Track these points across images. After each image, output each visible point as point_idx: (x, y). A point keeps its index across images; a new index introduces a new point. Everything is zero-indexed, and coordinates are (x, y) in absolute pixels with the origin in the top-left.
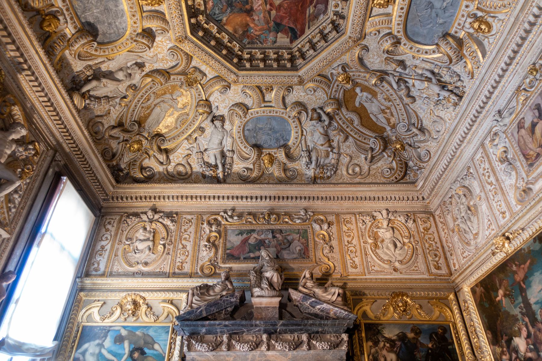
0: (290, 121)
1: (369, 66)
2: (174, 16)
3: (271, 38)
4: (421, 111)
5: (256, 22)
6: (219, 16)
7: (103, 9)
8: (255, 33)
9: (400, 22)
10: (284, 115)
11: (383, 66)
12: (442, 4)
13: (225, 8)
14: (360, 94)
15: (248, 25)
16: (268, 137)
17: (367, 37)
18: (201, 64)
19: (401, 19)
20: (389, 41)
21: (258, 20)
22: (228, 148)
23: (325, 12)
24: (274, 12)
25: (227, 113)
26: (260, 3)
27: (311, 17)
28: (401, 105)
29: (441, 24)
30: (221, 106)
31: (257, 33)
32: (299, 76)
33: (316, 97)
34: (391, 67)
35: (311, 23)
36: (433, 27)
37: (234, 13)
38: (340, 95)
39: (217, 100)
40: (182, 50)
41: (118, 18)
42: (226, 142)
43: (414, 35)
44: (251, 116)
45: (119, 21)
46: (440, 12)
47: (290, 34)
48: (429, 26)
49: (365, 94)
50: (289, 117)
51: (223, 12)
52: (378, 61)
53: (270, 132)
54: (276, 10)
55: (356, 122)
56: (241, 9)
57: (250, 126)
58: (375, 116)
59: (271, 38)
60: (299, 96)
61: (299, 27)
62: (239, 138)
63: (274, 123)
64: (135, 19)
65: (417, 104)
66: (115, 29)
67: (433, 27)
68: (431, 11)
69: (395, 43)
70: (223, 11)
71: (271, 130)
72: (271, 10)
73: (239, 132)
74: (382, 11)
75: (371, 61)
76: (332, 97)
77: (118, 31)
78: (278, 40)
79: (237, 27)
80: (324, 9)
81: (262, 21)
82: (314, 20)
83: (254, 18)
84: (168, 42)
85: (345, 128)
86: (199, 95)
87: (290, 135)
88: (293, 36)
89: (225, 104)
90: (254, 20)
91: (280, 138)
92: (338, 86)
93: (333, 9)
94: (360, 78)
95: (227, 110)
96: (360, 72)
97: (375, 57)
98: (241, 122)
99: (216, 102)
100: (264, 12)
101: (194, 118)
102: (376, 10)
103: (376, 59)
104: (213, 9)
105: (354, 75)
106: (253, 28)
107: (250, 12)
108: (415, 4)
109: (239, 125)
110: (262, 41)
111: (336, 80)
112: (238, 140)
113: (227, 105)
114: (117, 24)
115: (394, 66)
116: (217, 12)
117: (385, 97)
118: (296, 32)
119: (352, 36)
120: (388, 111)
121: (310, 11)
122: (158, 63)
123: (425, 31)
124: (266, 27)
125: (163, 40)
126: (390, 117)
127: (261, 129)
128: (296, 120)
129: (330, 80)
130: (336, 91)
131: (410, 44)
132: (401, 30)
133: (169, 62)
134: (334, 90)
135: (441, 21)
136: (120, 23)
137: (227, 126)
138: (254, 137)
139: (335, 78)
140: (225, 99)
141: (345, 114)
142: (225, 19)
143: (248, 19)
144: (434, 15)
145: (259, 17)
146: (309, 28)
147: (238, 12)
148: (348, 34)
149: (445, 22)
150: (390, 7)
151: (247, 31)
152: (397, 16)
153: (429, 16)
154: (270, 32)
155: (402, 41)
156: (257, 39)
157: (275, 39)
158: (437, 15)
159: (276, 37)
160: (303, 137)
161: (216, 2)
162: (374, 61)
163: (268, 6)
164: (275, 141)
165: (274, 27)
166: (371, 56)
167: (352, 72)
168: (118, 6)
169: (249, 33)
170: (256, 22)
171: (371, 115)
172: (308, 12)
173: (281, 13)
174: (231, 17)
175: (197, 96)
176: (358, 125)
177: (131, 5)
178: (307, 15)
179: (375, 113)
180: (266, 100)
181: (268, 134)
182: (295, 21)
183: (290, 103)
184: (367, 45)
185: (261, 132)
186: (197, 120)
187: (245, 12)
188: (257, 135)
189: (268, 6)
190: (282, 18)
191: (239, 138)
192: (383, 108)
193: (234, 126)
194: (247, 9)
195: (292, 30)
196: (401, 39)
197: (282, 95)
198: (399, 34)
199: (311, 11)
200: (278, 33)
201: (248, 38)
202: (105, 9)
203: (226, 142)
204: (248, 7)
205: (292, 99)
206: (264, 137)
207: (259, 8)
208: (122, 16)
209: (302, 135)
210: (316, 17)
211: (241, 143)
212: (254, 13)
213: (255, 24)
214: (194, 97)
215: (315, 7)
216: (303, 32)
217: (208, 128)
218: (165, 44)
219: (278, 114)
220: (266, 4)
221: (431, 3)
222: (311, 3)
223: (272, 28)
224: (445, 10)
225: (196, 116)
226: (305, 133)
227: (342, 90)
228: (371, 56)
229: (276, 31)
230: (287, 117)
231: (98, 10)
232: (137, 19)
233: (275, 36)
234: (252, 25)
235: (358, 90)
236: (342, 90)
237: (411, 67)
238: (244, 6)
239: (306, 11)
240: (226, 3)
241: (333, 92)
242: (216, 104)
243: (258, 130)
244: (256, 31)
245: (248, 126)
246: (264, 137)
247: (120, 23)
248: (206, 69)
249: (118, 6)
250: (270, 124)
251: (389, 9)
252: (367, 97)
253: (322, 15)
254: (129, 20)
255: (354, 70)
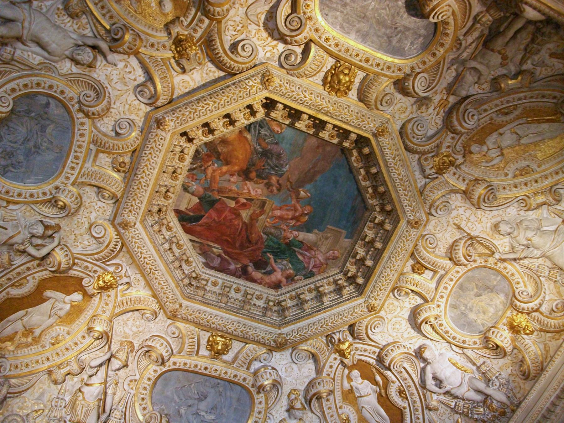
0: (48, 187)
1: (120, 318)
2: (306, 94)
3: (194, 186)
4: (37, 395)
5: (227, 177)
6: (255, 132)
7: (368, 14)
8: (210, 168)
9: (188, 366)
10: (62, 179)
11: (119, 338)
12: (203, 411)
13: (264, 145)
14: (68, 298)
15: (227, 164)
16: (21, 138)
17: (170, 321)
18: (205, 75)
19: (192, 366)
20: (167, 354)
21: (229, 181)
22: (18, 52)
23: (207, 265)
24: (232, 204)
25: (95, 76)
26: (252, 192)
27: (206, 247)
28: (47, 364)
29: (179, 412)
30: (115, 72)
31: (210, 171)
32: (135, 224)
33: (81, 235)
34: (115, 347)
35: (198, 245)
36: (175, 402)
37: (252, 154)
38: (74, 272)
39: (128, 70)
40: (248, 69)
41: (344, 20)
42: (33, 52)
43: (165, 379)
44: (77, 122)
45: (340, 18)
46: (194, 409)
47: (191, 214)
48: (176, 398)
49: (68, 307)
50: (57, 188)
51: (259, 138)
52: (127, 331)
53: (31, 144)
54: (234, 208)
55: (15, 292)
56: (254, 165)
57: (55, 110)
58: (21, 319)
59: (194, 186)
60: (92, 209)
61: (198, 229)
62: (38, 85)
63: (49, 156)
64: (332, 43)
65: (49, 387)
66: (335, 6)
67: (175, 402)
68: (195, 399)
69: (163, 359)
70: (261, 141)
71: (35, 146)
72: (236, 203)
73: (51, 87)
74: (204, 342)
75: (128, 322)
76: (76, 261)
77: (328, 7)
78: (188, 195)
79: (231, 147)
80: (211, 265)
81: (225, 185)
82: (200, 249)
83: (234, 177)
84: (268, 55)
85: (9, 276)
86: (152, 45)
87: (16, 178)
88: (187, 217)
89: (115, 80)
90: (232, 175)
91: (14, 160)
92: (95, 272)
93: (212, 279)
94: (102, 304)
95: (102, 78)
96: (115, 307)
97: (134, 329)
98: (71, 99)
99: (126, 66)
100: (237, 193)
101: (109, 11)
102: (205, 336)
103: (131, 329)
104: (269, 128)
105: (109, 296)
106: (219, 168)
107: (245, 174)
108: (206, 381)
109: (67, 92)
110: (194, 172)
111: (105, 270)
112: (35, 79)
113: (113, 84)
114: (338, 13)
115: (122, 356)
116: (263, 132)
117: (60, 338)
118: (191, 222)
119: (183, 308)
120: (30, 339)
121: (215, 248)
122: (244, 16)
123: (169, 393)
124: (215, 186)
125: (275, 51)
126: (16, 342)
127: (43, 129)
128: (48, 197)
129: (108, 261)
130: (87, 267)
131: (153, 376)
132: (177, 367)
133: (234, 33)
134: (90, 265)
135: (182, 411)
136: (336, 18)
137: (67, 67)
138: (28, 112)
139: (111, 269)
140: (125, 84)
141: (36, 275)
142: (249, 137)
143: (236, 168)
144: (190, 402)
145: (234, 183)
146: (191, 240)
147: (252, 159)
148: (185, 303)
149: (181, 416)
150: (207, 353)
151: (218, 159)
152: (196, 362)
153: (190, 397)
154: (205, 189)
155: (161, 367)
156: (201, 166)
157: (191, 191)
158: (190, 406)
159: (193, 194)
160: (5, 204)
161: (276, 136)
162: (128, 326)
163: (245, 201)
164: (8, 150)
165: (210, 197)
166: (138, 323)
167: (116, 296)
168: (357, 32)
169: (214, 159)
170: (227, 177)
171: (22, 313)
172: (216, 245)
173: (227, 213)
174: (248, 147)
175: (152, 40)
176: (8, 293)
177: (350, 52)
178: (212, 244)
179: (25, 319)
180: (101, 155)
181: (27, 140)
182: (209, 227)
183: (81, 192)
184: (157, 320)
185: (37, 128)
186: (104, 15)
187: (247, 169)
188: (33, 118)
189: (245, 201)
190: (220, 212)
191: (38, 85)
192: (37, 332)
193: (63, 78)
194: (251, 172)
195: (197, 219)
196: (164, 366)
197: (108, 188)
198: (171, 364)
199: (215, 250)
200: (199, 199)
201: (206, 155)
202: (365, 16)
203: (33, 52)
204: (253, 175)
205: (89, 198)
206: (22, 130)
207: (246, 187)
208: (342, 27)
209: (9, 202)
210: (204, 252)
211: (26, 86)
212: (241, 179)
213: (225, 173)
214: (150, 32)
215: (219, 256)
216: (187, 231)
217: (76, 27)
218: (268, 48)
219: (67, 169)
220: (247, 199)
221: (206, 398)
222: (225, 252)
223: (210, 194)
224: (197, 414)
225: (111, 17)
226: (11, 207)
227: (84, 275)
228: (138, 323)
229: (202, 198)
230: (57, 183)
231: (370, 8)
232: (330, 46)
233: (195, 193)
234: (225, 169)
235: (77, 297)
236: (84, 275)
237: (117, 377)
238: (257, 171)
239: (218, 244)
240: (270, 150)
241: (86, 264)
242: (121, 65)
243: (43, 122)
244: (214, 171)
245: (57, 106)
246: (22, 130)
247: (336, 18)
248: (193, 80)
249: (357, 32)
250: (48, 149)
251: (204, 352)
252: (61, 309)
253: (204, 261)
254: (334, 34)
255: (119, 298)
